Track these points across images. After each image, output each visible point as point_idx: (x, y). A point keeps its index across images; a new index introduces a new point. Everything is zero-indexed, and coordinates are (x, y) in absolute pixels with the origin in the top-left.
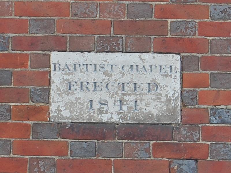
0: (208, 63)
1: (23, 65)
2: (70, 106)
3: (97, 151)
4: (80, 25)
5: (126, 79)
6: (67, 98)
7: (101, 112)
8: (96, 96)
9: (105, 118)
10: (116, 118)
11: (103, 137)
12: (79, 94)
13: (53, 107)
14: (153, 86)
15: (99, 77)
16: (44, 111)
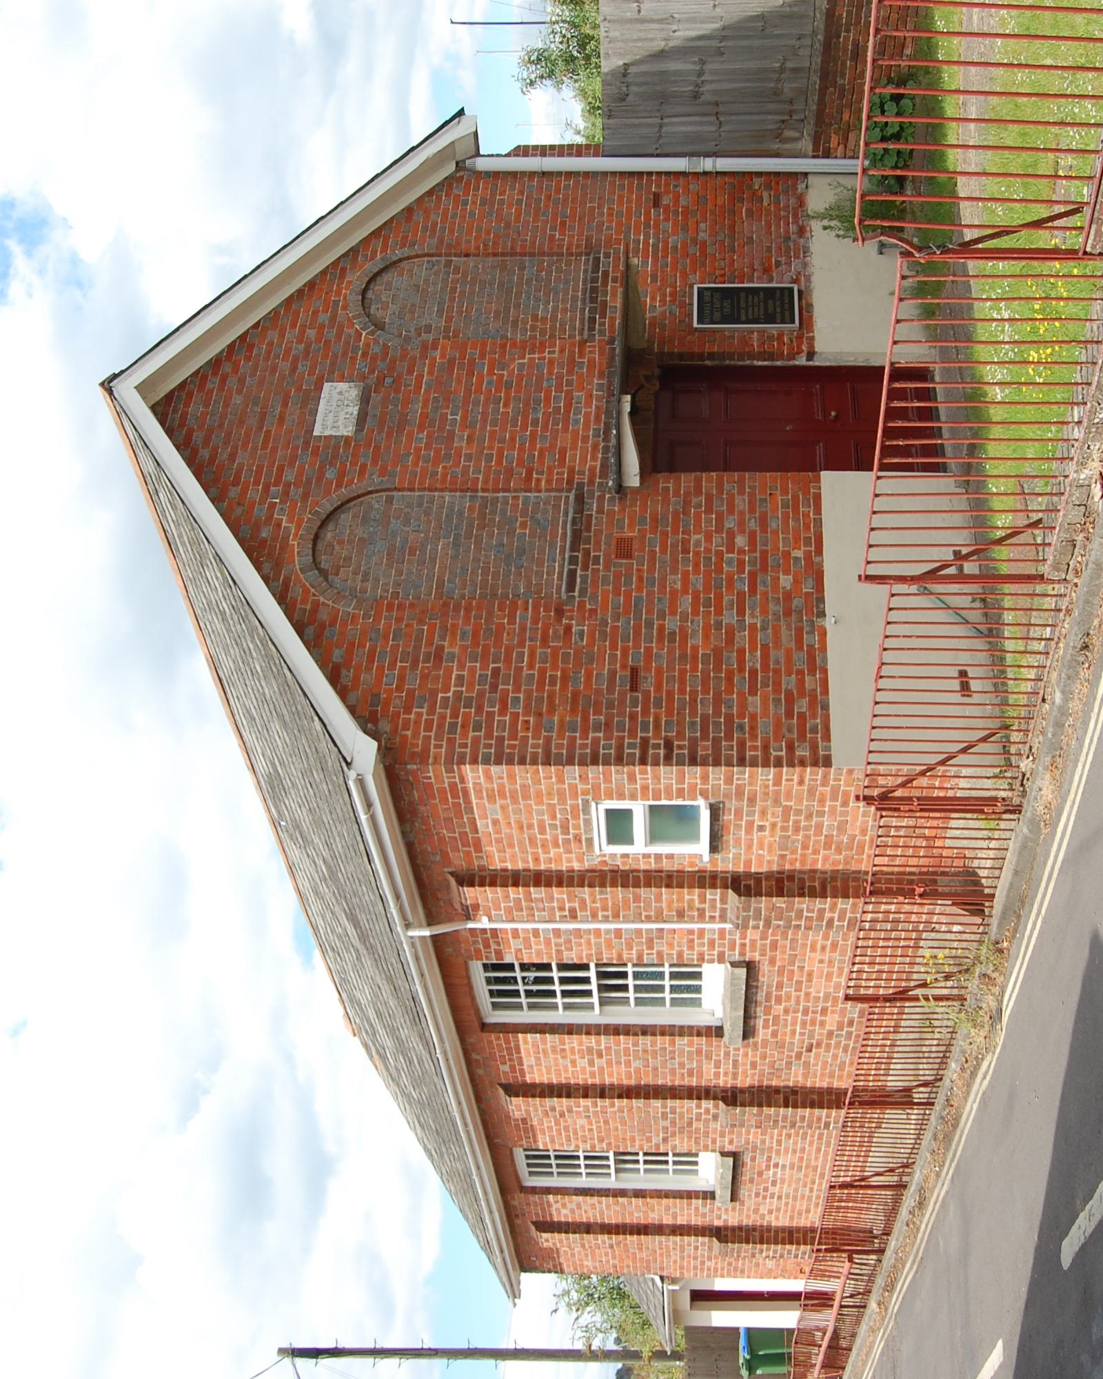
0: (331, 372)
1: (319, 447)
2: (346, 427)
3: (375, 416)
4: (299, 423)
5: (335, 404)
6: (341, 428)
7: (352, 414)
8: (342, 416)
9: (356, 413)
10: (357, 408)
11: (367, 414)
12: (340, 423)
13: (346, 434)
14: (340, 393)
15: (331, 417)
16: (347, 440)
